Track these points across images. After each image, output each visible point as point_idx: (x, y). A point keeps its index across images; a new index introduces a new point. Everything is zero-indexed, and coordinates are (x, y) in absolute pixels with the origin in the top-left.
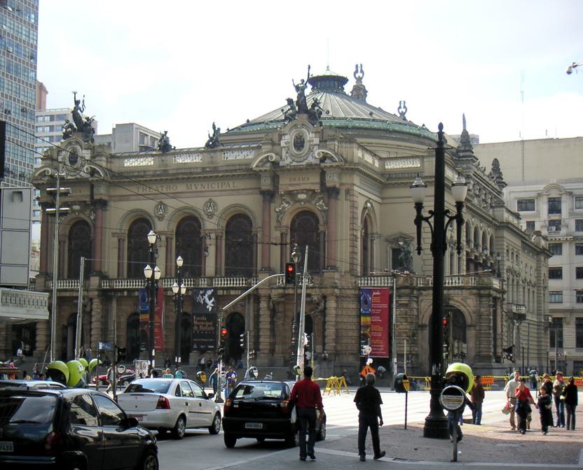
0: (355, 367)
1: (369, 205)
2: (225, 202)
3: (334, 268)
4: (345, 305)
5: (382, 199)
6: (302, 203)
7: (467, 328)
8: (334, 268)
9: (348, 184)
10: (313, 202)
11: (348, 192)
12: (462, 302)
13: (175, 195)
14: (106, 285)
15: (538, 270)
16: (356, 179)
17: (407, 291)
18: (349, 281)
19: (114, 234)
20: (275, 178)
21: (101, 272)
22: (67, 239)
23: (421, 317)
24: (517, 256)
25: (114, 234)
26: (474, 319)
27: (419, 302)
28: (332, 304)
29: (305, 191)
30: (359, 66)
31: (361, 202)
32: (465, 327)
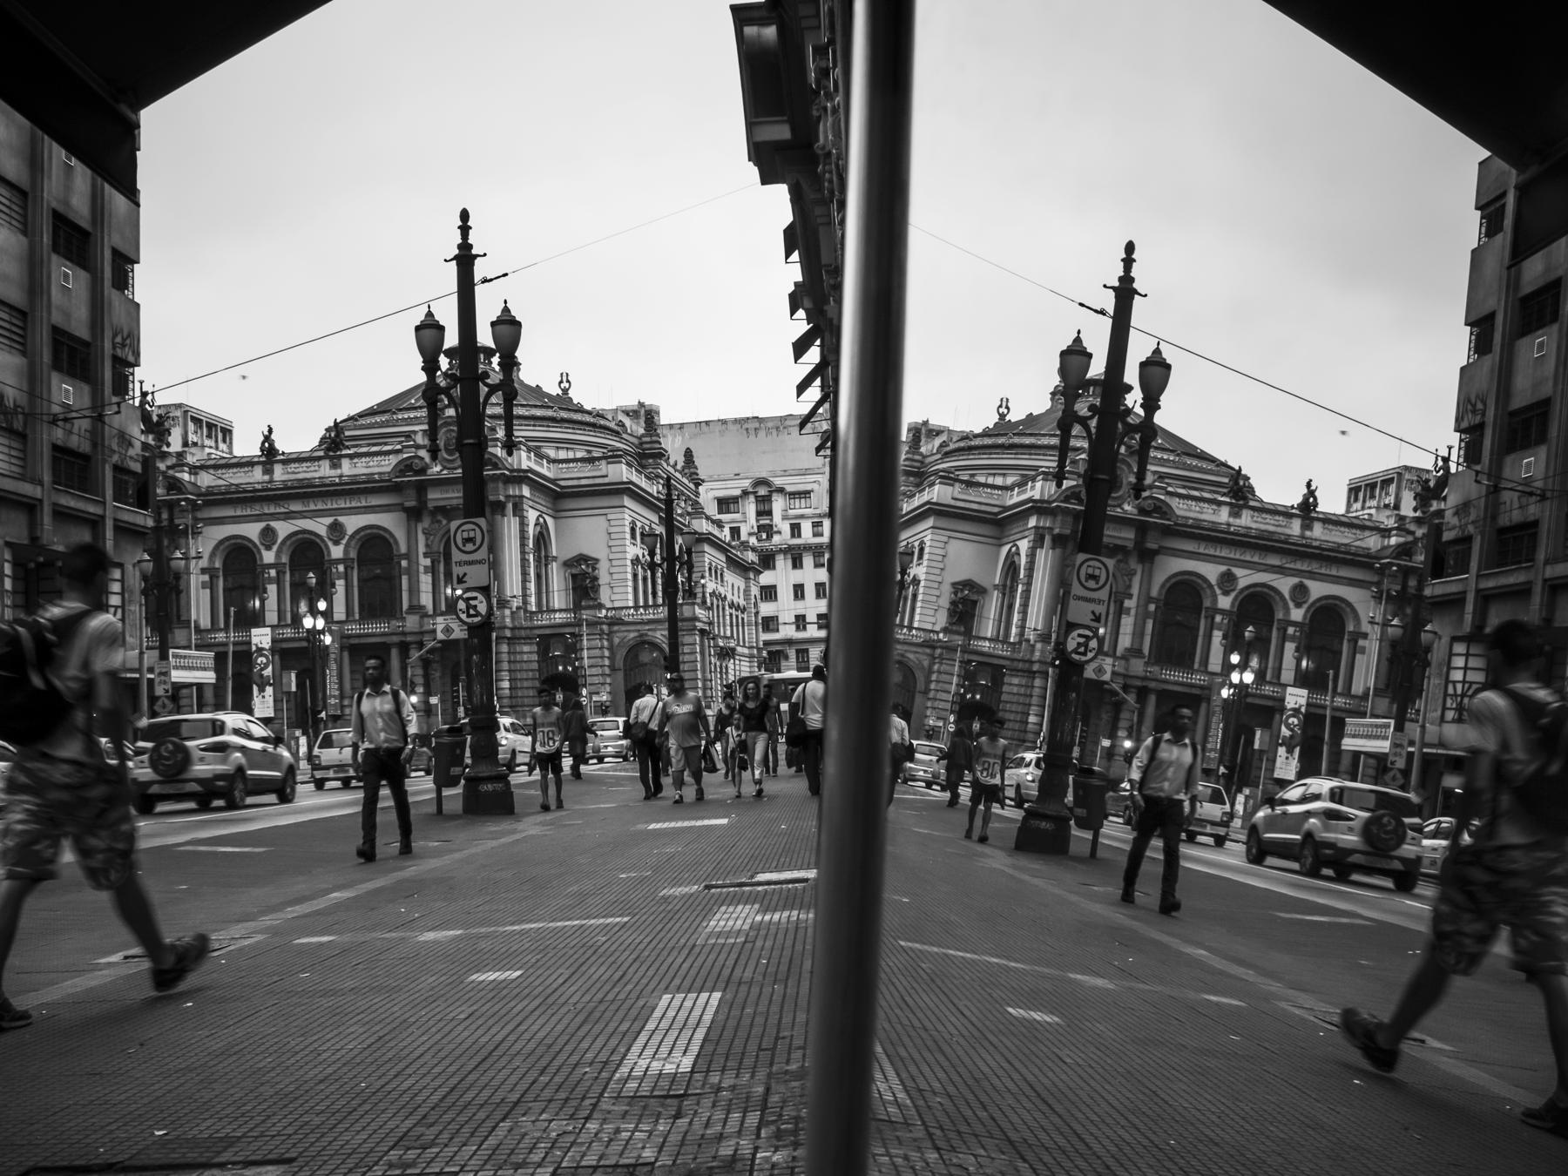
13: (288, 516)
15: (747, 591)
19: (203, 571)
25: (203, 571)
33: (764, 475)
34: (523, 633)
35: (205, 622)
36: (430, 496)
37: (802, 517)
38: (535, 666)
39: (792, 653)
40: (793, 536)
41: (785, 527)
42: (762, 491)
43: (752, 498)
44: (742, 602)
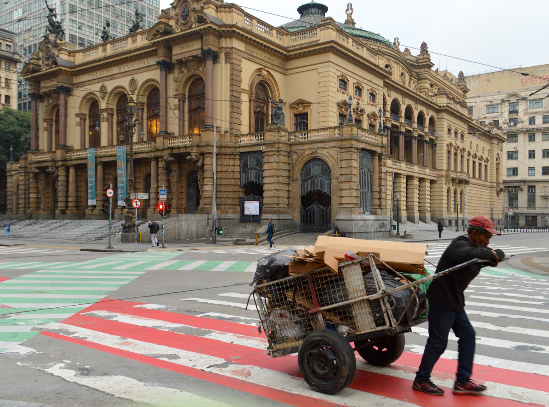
0: (235, 219)
1: (264, 73)
2: (141, 78)
4: (225, 162)
9: (227, 48)
13: (111, 77)
15: (490, 151)
16: (237, 44)
19: (77, 115)
20: (169, 50)
21: (65, 146)
24: (462, 136)
25: (77, 115)
30: (350, 5)
31: (248, 70)
33: (515, 91)
34: (228, 151)
35: (77, 146)
36: (174, 52)
37: (537, 113)
38: (237, 175)
39: (525, 188)
40: (530, 123)
41: (526, 119)
42: (513, 100)
43: (507, 104)
44: (485, 157)
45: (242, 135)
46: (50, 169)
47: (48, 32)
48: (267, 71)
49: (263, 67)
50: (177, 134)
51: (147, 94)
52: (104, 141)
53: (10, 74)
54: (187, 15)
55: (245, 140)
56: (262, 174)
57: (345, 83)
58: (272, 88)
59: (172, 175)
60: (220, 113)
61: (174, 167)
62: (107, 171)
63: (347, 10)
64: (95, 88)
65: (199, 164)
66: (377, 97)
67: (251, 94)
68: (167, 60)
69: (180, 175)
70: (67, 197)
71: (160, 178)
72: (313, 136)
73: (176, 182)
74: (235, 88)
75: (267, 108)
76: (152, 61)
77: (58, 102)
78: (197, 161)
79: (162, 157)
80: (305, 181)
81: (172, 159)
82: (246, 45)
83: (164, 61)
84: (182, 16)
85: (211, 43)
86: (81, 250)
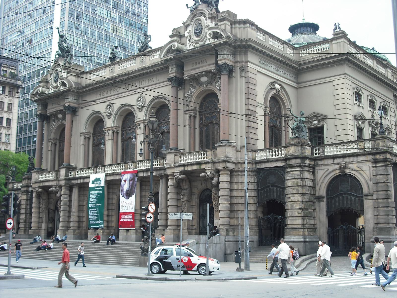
1: (277, 86)
3: (228, 144)
5: (298, 83)
6: (205, 86)
7: (364, 197)
8: (228, 144)
9: (242, 62)
10: (214, 84)
11: (243, 69)
12: (358, 169)
14: (72, 175)
17: (298, 161)
18: (245, 156)
22: (58, 142)
23: (317, 188)
26: (370, 187)
27: (316, 173)
28: (224, 178)
29: (203, 73)
32: (362, 197)
45: (260, 150)
46: (54, 189)
47: (57, 56)
48: (280, 85)
49: (276, 81)
50: (187, 150)
51: (199, 102)
52: (108, 160)
53: (12, 99)
54: (201, 32)
55: (261, 156)
56: (284, 192)
57: (360, 96)
58: (286, 103)
59: (182, 193)
60: (234, 128)
61: (185, 186)
62: (111, 190)
63: (335, 29)
64: (101, 108)
65: (215, 181)
66: (389, 109)
67: (266, 108)
68: (178, 76)
69: (191, 194)
70: (69, 217)
71: (169, 197)
72: (330, 151)
73: (187, 201)
74: (251, 102)
75: (280, 122)
76: (162, 78)
77: (64, 122)
78: (212, 179)
79: (173, 175)
80: (332, 198)
81: (183, 176)
82: (259, 58)
83: (176, 77)
84: (195, 33)
85: (225, 58)
86: (117, 277)
